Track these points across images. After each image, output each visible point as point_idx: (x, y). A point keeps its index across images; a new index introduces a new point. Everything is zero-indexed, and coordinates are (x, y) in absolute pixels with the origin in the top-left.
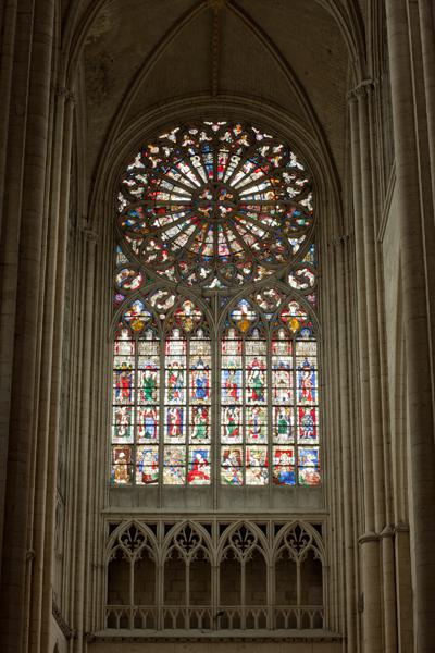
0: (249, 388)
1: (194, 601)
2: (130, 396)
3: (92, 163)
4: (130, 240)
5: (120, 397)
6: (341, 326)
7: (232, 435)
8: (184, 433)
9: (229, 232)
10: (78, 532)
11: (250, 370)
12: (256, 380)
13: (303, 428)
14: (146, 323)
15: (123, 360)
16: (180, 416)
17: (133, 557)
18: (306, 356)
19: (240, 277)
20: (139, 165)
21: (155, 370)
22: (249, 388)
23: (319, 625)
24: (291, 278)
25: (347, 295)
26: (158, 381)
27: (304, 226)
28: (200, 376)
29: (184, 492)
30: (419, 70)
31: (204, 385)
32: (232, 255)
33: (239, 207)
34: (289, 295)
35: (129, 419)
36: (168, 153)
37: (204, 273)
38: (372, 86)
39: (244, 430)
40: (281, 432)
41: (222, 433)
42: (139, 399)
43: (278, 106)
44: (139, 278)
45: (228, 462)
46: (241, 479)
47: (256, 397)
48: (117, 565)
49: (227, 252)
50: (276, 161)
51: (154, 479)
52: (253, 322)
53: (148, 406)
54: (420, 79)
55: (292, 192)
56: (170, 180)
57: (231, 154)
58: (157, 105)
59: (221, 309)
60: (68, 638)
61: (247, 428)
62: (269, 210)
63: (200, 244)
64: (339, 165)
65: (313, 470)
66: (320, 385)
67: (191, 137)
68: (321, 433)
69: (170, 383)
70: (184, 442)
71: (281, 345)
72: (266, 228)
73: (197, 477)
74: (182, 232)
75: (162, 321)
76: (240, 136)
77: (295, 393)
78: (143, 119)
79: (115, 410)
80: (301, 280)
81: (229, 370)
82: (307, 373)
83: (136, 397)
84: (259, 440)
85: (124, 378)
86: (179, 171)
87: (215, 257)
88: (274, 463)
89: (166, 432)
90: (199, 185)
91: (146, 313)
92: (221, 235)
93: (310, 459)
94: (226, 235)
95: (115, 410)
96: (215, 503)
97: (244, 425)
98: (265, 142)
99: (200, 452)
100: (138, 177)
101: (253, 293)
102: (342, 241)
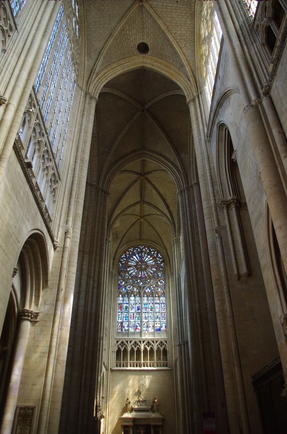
1: (137, 360)
3: (114, 255)
5: (119, 310)
7: (145, 319)
8: (134, 319)
9: (145, 272)
10: (109, 343)
12: (151, 306)
15: (120, 302)
16: (133, 315)
17: (122, 349)
18: (162, 301)
19: (147, 282)
20: (124, 256)
23: (167, 366)
24: (159, 282)
27: (162, 270)
28: (138, 305)
29: (134, 333)
30: (189, 235)
32: (146, 276)
33: (147, 266)
34: (157, 286)
35: (121, 316)
36: (131, 253)
37: (139, 281)
38: (177, 239)
43: (156, 243)
44: (124, 282)
47: (151, 310)
48: (118, 352)
49: (144, 276)
50: (155, 255)
53: (126, 312)
54: (189, 238)
56: (131, 260)
57: (145, 254)
58: (128, 243)
59: (143, 289)
60: (106, 370)
62: (154, 267)
64: (170, 256)
67: (136, 250)
71: (157, 298)
74: (134, 272)
75: (129, 292)
76: (147, 250)
78: (125, 246)
80: (161, 283)
84: (152, 321)
86: (133, 258)
90: (138, 261)
91: (125, 291)
92: (143, 272)
93: (164, 325)
94: (144, 272)
96: (141, 336)
98: (153, 251)
99: (138, 323)
100: (124, 259)
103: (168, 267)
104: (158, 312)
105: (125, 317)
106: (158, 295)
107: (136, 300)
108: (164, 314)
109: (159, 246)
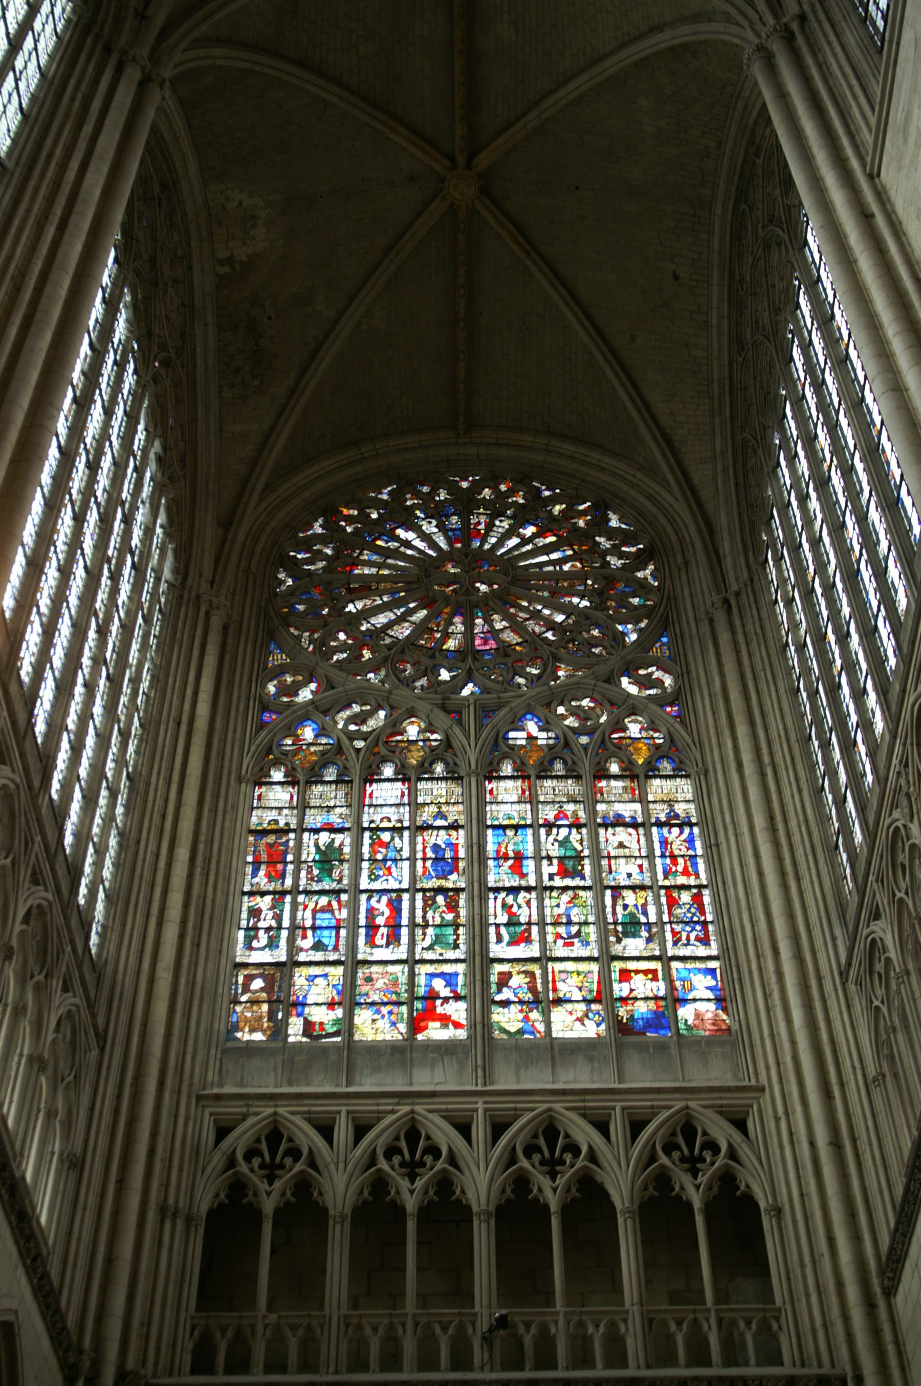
0: (549, 858)
2: (283, 876)
4: (296, 633)
5: (262, 880)
6: (742, 730)
7: (513, 942)
8: (405, 939)
11: (549, 826)
12: (565, 843)
13: (678, 928)
14: (323, 753)
15: (272, 815)
19: (521, 681)
21: (341, 830)
22: (549, 858)
25: (749, 676)
26: (347, 850)
28: (441, 838)
31: (448, 854)
32: (505, 649)
35: (278, 918)
37: (445, 675)
39: (543, 934)
40: (626, 934)
41: (493, 937)
42: (303, 882)
44: (313, 686)
45: (506, 994)
46: (541, 1027)
47: (564, 872)
49: (492, 644)
51: (330, 1029)
52: (550, 747)
55: (615, 562)
61: (549, 929)
63: (438, 635)
64: (706, 493)
65: (712, 1006)
66: (707, 846)
68: (722, 934)
69: (374, 852)
70: (404, 957)
71: (613, 783)
72: (569, 610)
73: (431, 1024)
75: (358, 751)
77: (653, 866)
79: (246, 903)
81: (504, 828)
82: (676, 831)
83: (296, 878)
84: (578, 950)
85: (269, 846)
86: (397, 539)
87: (467, 652)
88: (617, 993)
89: (361, 940)
93: (702, 985)
94: (488, 621)
95: (246, 903)
97: (542, 924)
99: (442, 975)
101: (549, 705)
102: (726, 601)
103: (702, 574)
104: (633, 888)
105: (314, 928)
106: (621, 762)
107: (420, 800)
108: (697, 899)
109: (608, 461)
